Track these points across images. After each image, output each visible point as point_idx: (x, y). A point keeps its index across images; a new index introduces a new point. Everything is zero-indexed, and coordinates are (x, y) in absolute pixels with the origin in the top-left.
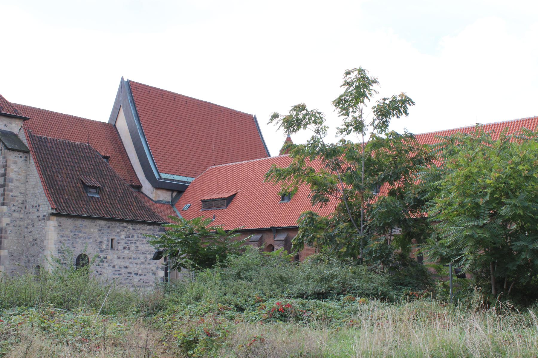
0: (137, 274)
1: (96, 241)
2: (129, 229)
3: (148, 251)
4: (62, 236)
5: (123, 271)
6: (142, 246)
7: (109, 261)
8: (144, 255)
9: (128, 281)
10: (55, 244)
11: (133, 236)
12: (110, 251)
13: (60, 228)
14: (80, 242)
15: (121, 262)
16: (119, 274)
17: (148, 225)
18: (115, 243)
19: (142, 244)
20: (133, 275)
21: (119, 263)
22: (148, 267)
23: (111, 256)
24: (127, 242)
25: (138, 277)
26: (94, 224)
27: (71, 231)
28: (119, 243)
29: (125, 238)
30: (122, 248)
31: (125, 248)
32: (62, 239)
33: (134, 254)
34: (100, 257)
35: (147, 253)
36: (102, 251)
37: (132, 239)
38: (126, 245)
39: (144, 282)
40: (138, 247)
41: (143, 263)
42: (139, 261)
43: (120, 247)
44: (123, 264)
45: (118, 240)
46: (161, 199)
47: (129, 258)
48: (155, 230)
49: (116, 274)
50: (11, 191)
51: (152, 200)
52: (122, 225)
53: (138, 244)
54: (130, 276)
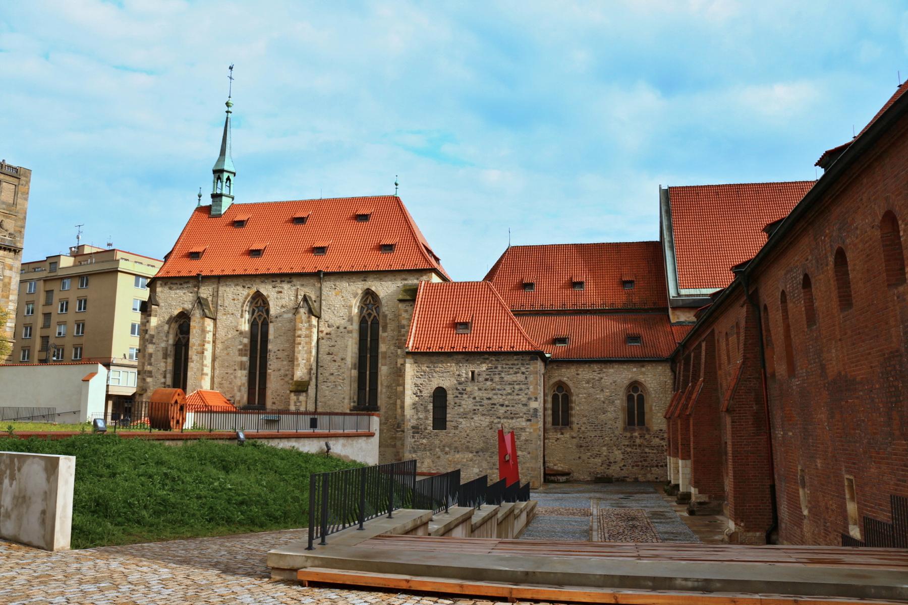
2: (492, 360)
4: (417, 372)
5: (485, 402)
6: (508, 376)
8: (511, 386)
9: (491, 412)
11: (496, 368)
12: (469, 383)
16: (480, 406)
19: (508, 375)
20: (498, 406)
21: (481, 395)
24: (490, 373)
25: (504, 409)
27: (428, 367)
28: (479, 375)
29: (487, 369)
31: (486, 380)
32: (418, 374)
33: (498, 385)
35: (515, 383)
36: (460, 384)
37: (496, 370)
39: (511, 413)
40: (503, 378)
41: (510, 394)
42: (505, 392)
44: (485, 395)
47: (493, 390)
50: (404, 336)
52: (483, 357)
53: (503, 375)
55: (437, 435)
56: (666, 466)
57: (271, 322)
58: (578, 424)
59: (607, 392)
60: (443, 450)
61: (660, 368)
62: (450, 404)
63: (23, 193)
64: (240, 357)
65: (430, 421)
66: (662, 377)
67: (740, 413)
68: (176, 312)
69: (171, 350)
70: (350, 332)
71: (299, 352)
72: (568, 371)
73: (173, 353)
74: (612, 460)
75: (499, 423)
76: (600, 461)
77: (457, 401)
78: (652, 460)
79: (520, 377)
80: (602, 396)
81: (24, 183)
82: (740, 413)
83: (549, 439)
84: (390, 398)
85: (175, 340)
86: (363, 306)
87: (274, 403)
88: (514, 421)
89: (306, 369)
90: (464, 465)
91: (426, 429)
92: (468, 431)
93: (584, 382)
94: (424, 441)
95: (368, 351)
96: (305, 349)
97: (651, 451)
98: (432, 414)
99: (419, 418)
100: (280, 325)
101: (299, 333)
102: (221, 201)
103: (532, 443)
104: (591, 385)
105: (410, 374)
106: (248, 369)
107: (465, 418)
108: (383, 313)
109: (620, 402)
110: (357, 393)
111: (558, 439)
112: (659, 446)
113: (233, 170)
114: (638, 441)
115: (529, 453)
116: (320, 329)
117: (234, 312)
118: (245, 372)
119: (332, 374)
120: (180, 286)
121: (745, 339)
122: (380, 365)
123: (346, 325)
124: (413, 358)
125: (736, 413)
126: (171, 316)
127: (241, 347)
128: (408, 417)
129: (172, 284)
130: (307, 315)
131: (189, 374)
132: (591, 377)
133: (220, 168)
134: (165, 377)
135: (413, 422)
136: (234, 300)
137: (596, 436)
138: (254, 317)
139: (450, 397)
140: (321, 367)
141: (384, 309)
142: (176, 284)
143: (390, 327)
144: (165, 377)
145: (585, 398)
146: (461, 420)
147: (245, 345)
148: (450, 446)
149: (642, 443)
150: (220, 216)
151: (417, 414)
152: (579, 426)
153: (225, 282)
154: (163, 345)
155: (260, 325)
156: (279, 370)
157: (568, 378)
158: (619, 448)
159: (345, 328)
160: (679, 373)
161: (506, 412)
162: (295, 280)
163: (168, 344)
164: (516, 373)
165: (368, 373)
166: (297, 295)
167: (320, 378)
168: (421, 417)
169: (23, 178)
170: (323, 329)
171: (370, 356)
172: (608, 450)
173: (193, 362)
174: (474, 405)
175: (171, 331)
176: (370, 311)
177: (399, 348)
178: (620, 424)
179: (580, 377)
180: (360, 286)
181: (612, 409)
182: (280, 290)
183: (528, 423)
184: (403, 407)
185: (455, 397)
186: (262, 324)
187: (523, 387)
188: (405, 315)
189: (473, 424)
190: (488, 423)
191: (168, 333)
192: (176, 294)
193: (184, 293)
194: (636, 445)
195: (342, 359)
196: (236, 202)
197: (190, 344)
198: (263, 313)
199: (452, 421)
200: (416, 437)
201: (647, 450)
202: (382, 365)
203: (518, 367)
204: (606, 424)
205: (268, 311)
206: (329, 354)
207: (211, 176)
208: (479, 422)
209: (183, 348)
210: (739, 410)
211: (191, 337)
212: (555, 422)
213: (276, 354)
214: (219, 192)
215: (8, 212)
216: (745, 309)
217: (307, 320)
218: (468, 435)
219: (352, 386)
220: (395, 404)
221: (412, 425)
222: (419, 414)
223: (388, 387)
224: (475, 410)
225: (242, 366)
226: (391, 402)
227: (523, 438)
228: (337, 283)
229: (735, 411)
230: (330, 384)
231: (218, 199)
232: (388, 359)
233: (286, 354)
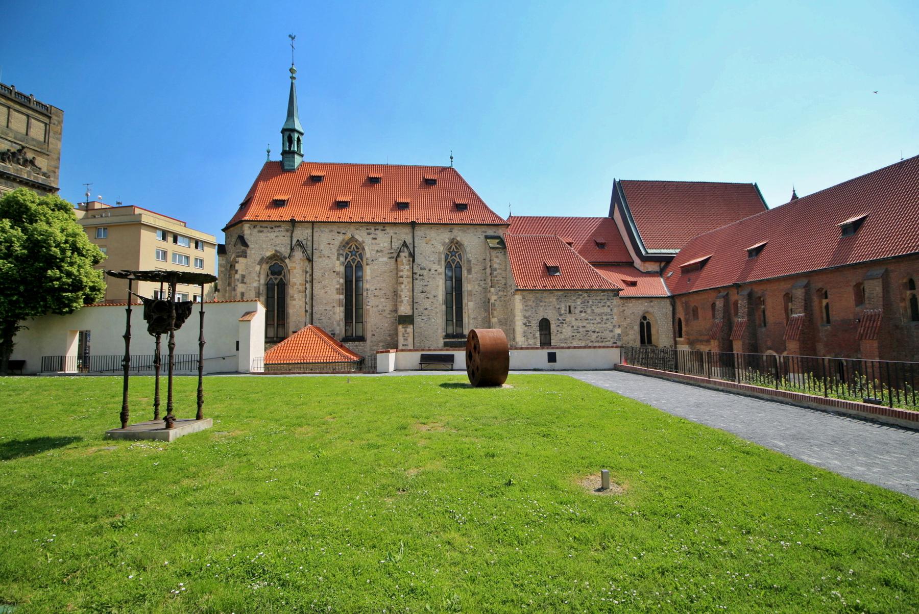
0: (594, 332)
1: (555, 307)
4: (526, 306)
7: (568, 323)
8: (601, 317)
9: (585, 337)
11: (588, 302)
12: (568, 315)
14: (541, 309)
18: (572, 309)
21: (577, 324)
22: (604, 326)
23: (569, 318)
25: (596, 335)
26: (551, 295)
31: (581, 312)
32: (527, 308)
36: (561, 315)
40: (593, 310)
41: (600, 323)
42: (595, 322)
43: (577, 311)
44: (581, 325)
46: (650, 270)
50: (496, 277)
51: (641, 272)
53: (593, 308)
57: (367, 265)
59: (628, 320)
63: (55, 133)
64: (338, 296)
68: (268, 254)
69: (263, 289)
70: (439, 274)
71: (402, 291)
73: (265, 292)
77: (559, 329)
79: (606, 310)
81: (56, 123)
87: (373, 335)
89: (409, 305)
96: (407, 287)
101: (401, 274)
102: (294, 158)
108: (467, 258)
109: (637, 328)
113: (301, 130)
117: (330, 255)
118: (342, 309)
120: (270, 230)
123: (436, 269)
124: (521, 294)
126: (263, 258)
127: (338, 286)
129: (261, 227)
130: (407, 258)
133: (290, 127)
136: (329, 244)
139: (553, 327)
142: (267, 227)
150: (292, 171)
153: (319, 227)
154: (255, 284)
155: (354, 267)
156: (377, 306)
159: (436, 271)
162: (388, 229)
163: (260, 284)
164: (604, 306)
168: (531, 343)
169: (54, 117)
170: (416, 271)
175: (262, 272)
176: (454, 257)
180: (448, 236)
182: (374, 237)
186: (356, 267)
187: (609, 317)
192: (267, 237)
195: (435, 297)
196: (307, 159)
198: (356, 256)
206: (423, 292)
215: (39, 150)
228: (428, 232)
230: (425, 317)
232: (473, 296)
233: (383, 292)
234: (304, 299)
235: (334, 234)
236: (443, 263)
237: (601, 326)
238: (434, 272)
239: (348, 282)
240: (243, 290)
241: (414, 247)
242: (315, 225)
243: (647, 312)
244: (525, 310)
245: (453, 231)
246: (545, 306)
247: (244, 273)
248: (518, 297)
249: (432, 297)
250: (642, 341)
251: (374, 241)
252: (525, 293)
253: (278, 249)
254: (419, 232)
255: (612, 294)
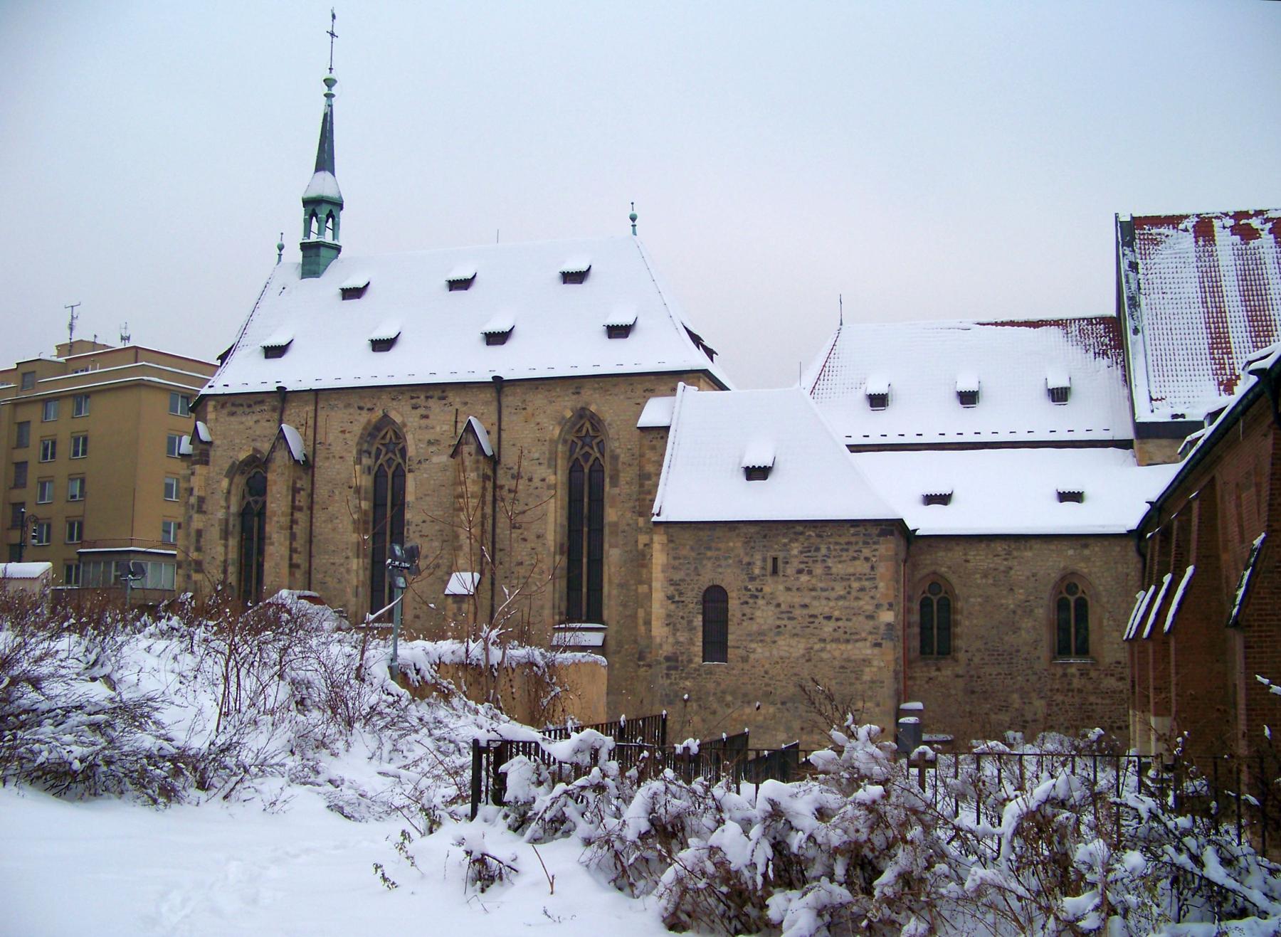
1: (741, 562)
2: (810, 536)
3: (854, 575)
4: (675, 558)
6: (840, 566)
8: (845, 583)
9: (808, 630)
10: (663, 572)
11: (818, 549)
12: (769, 579)
13: (672, 545)
15: (793, 597)
16: (790, 619)
17: (852, 526)
18: (780, 564)
19: (840, 562)
21: (789, 599)
24: (806, 560)
25: (832, 624)
28: (787, 563)
29: (801, 552)
30: (794, 572)
31: (800, 572)
32: (677, 563)
33: (821, 581)
34: (750, 590)
35: (852, 578)
36: (752, 579)
38: (802, 566)
39: (845, 633)
40: (829, 568)
42: (833, 595)
44: (797, 599)
45: (785, 558)
47: (813, 589)
48: (869, 535)
49: (783, 619)
52: (793, 530)
53: (830, 563)
54: (813, 622)
55: (711, 673)
56: (1127, 727)
57: (410, 471)
58: (967, 651)
59: (1020, 594)
60: (721, 700)
61: (1118, 549)
62: (733, 615)
65: (698, 648)
66: (1119, 566)
67: (1262, 631)
68: (242, 456)
72: (950, 555)
73: (238, 528)
74: (1029, 717)
75: (822, 650)
76: (1008, 719)
77: (747, 610)
78: (1102, 718)
80: (1010, 602)
82: (1262, 631)
83: (911, 678)
84: (624, 605)
85: (240, 506)
86: (575, 440)
87: (417, 617)
88: (850, 647)
90: (761, 727)
91: (690, 661)
92: (767, 666)
93: (978, 576)
94: (688, 683)
95: (585, 521)
97: (1099, 701)
98: (700, 634)
99: (678, 643)
100: (425, 475)
103: (882, 687)
104: (991, 581)
105: (660, 562)
106: (370, 555)
107: (761, 641)
110: (565, 598)
111: (930, 679)
112: (1114, 692)
114: (1076, 683)
115: (878, 705)
116: (499, 483)
117: (344, 454)
119: (521, 564)
120: (247, 410)
121: (1271, 494)
122: (606, 546)
123: (544, 475)
125: (1254, 632)
126: (234, 463)
128: (658, 640)
129: (233, 405)
131: (266, 566)
132: (991, 566)
134: (225, 572)
135: (667, 649)
136: (343, 432)
137: (999, 674)
138: (379, 462)
139: (734, 605)
140: (501, 550)
141: (613, 445)
142: (242, 405)
143: (624, 477)
144: (225, 572)
145: (980, 604)
146: (753, 645)
147: (366, 513)
148: (733, 693)
149: (1085, 686)
151: (674, 635)
152: (969, 654)
154: (221, 514)
157: (949, 567)
158: (1042, 695)
159: (543, 480)
160: (1152, 559)
161: (835, 630)
163: (228, 513)
164: (854, 559)
165: (585, 560)
166: (456, 422)
167: (500, 572)
168: (681, 639)
171: (589, 532)
172: (1022, 698)
173: (272, 544)
174: (779, 618)
176: (587, 449)
177: (641, 514)
178: (1044, 651)
179: (970, 565)
180: (569, 404)
181: (1029, 625)
183: (876, 650)
184: (648, 623)
185: (742, 604)
187: (867, 584)
188: (650, 455)
189: (775, 652)
190: (802, 652)
191: (229, 492)
193: (257, 422)
194: (1073, 691)
195: (538, 537)
197: (268, 513)
199: (738, 647)
200: (673, 677)
201: (1092, 699)
202: (610, 546)
203: (857, 548)
204: (1018, 651)
205: (403, 452)
207: (300, 212)
208: (787, 648)
209: (256, 519)
210: (1259, 626)
211: (269, 499)
212: (926, 649)
213: (419, 528)
214: (314, 238)
216: (1270, 440)
217: (474, 466)
218: (766, 672)
219: (557, 585)
220: (634, 617)
221: (665, 654)
222: (678, 634)
223: (621, 586)
224: (779, 627)
225: (359, 550)
226: (627, 613)
227: (866, 677)
229: (1250, 626)
231: (313, 252)
233: (437, 528)
234: (288, 543)
235: (352, 410)
236: (562, 463)
237: (847, 604)
238: (539, 484)
239: (378, 504)
240: (201, 526)
241: (500, 429)
242: (320, 396)
243: (1073, 573)
244: (673, 568)
245: (582, 391)
246: (717, 559)
247: (202, 494)
248: (659, 539)
249: (532, 537)
250: (1062, 649)
251: (424, 422)
252: (670, 530)
253: (258, 445)
254: (510, 398)
255: (875, 531)
